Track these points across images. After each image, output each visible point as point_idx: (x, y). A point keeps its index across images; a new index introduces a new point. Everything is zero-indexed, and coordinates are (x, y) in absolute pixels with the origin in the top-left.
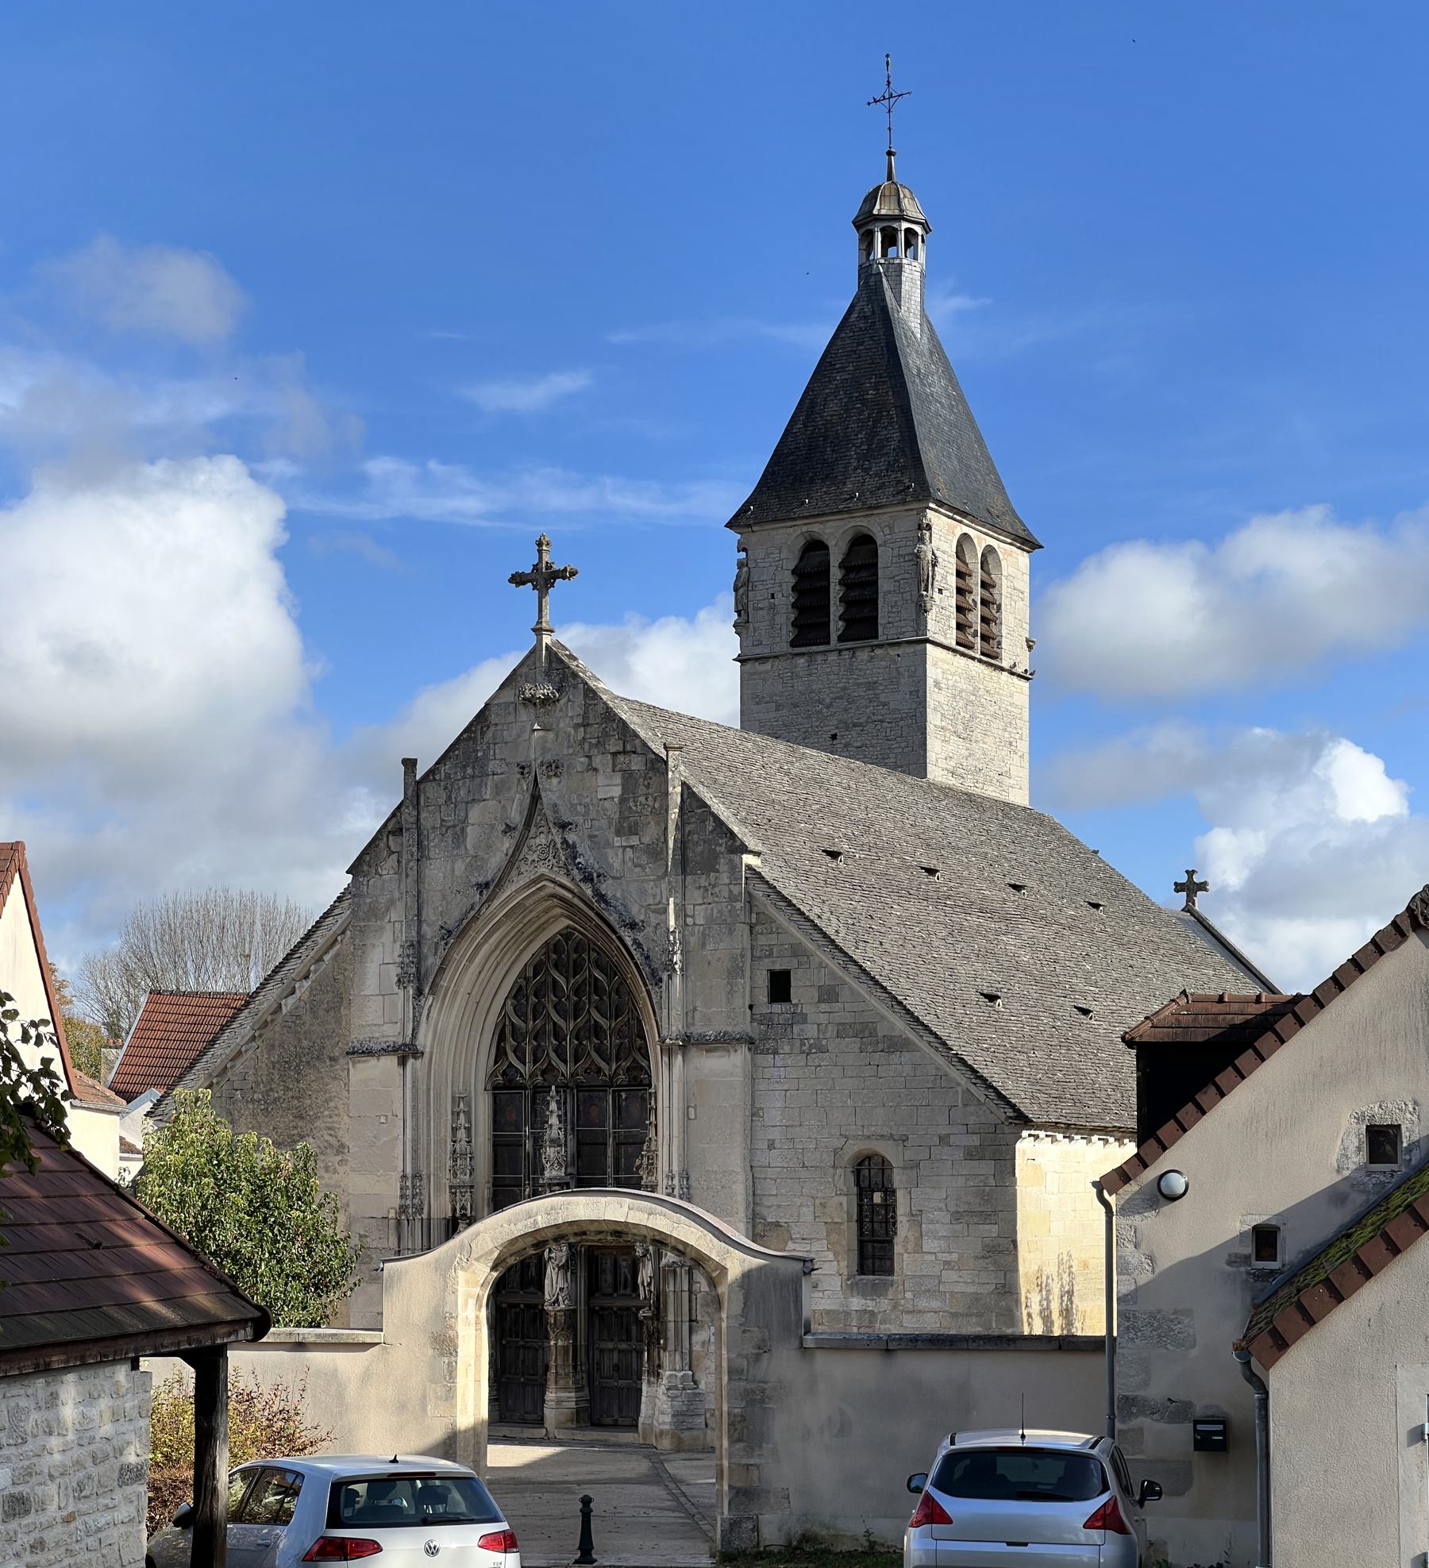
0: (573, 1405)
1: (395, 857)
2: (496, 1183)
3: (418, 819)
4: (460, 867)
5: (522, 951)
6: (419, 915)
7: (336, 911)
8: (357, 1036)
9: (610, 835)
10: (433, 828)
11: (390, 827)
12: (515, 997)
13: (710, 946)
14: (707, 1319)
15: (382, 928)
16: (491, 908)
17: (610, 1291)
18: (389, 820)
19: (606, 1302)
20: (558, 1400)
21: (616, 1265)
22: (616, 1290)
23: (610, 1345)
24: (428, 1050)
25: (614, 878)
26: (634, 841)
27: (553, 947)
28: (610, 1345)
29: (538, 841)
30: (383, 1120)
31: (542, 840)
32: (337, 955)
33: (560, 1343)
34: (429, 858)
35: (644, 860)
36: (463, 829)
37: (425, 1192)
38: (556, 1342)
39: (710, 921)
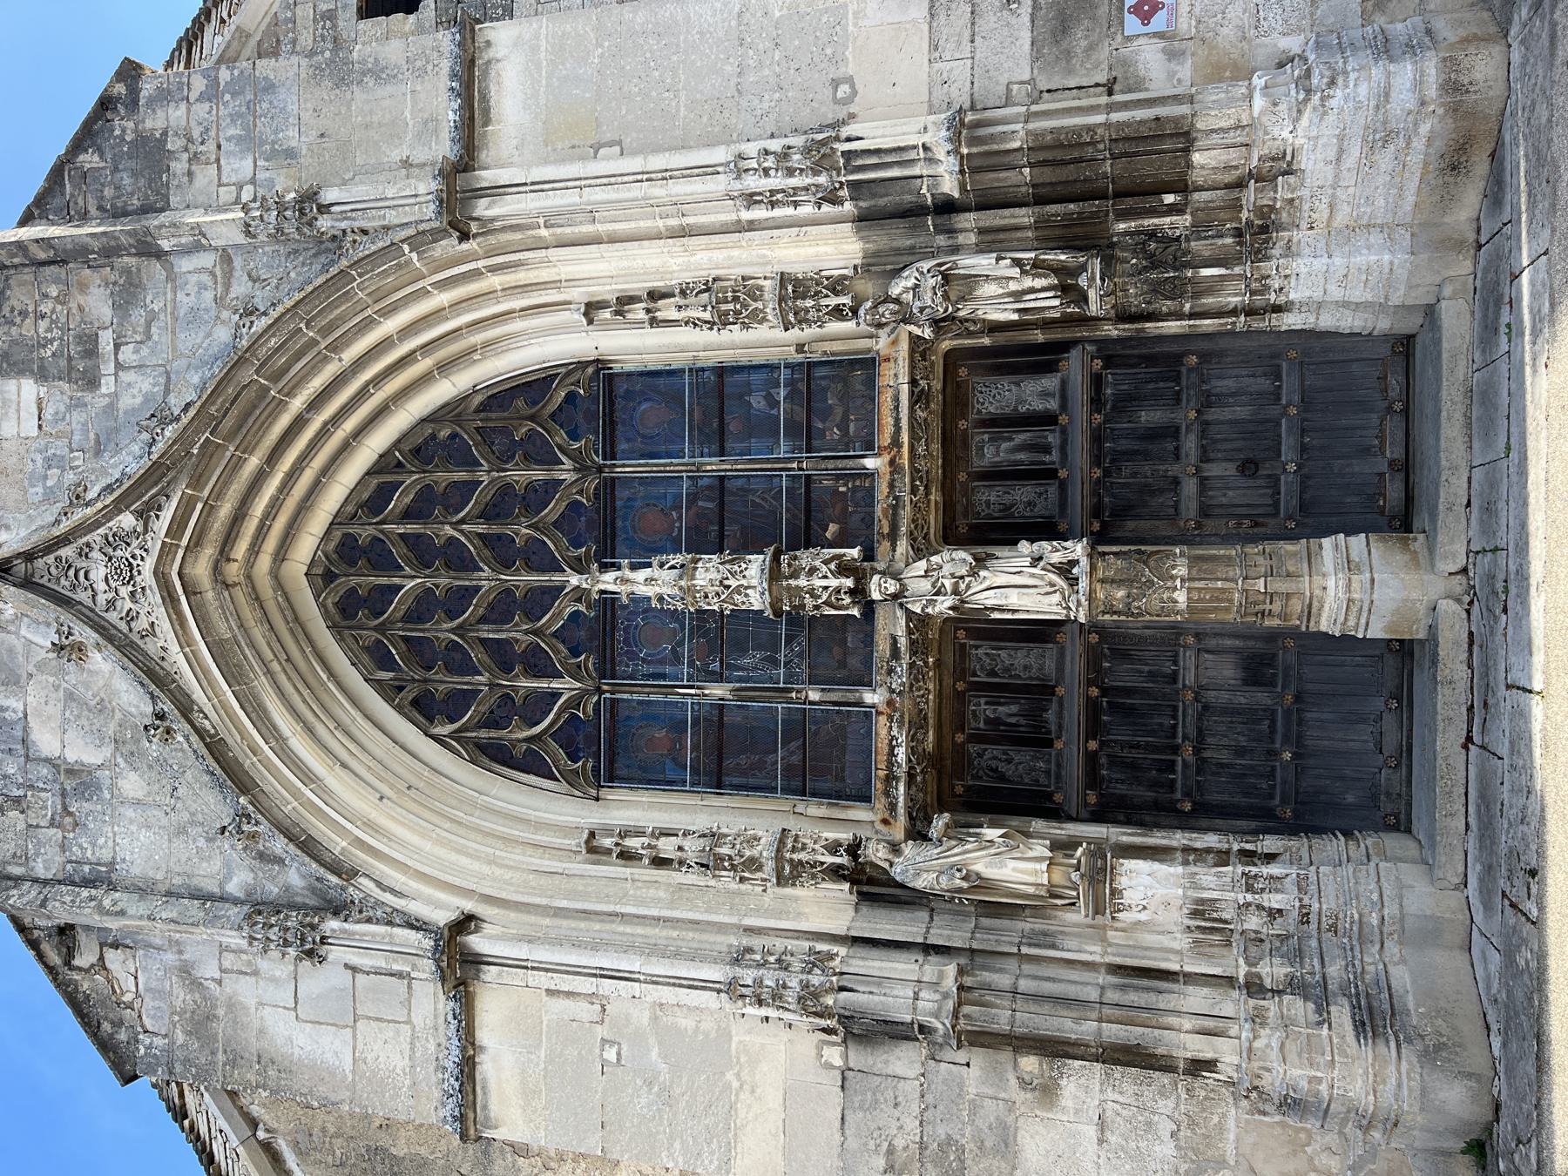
0: (1358, 542)
1: (111, 956)
2: (800, 784)
3: (45, 882)
4: (132, 784)
5: (332, 674)
6: (204, 897)
7: (203, 1130)
8: (423, 1102)
9: (97, 400)
10: (63, 848)
11: (55, 958)
12: (431, 720)
13: (291, 137)
14: (1104, 52)
15: (232, 1005)
16: (208, 709)
17: (1053, 491)
18: (41, 957)
19: (1079, 498)
20: (1346, 587)
21: (994, 475)
22: (1051, 474)
23: (1190, 487)
24: (469, 906)
25: (167, 391)
26: (106, 340)
27: (347, 613)
28: (1190, 487)
29: (101, 586)
30: (611, 1055)
31: (99, 573)
32: (295, 1145)
33: (1181, 571)
34: (112, 864)
35: (138, 316)
36: (71, 772)
37: (779, 944)
38: (1178, 588)
39: (249, 141)
